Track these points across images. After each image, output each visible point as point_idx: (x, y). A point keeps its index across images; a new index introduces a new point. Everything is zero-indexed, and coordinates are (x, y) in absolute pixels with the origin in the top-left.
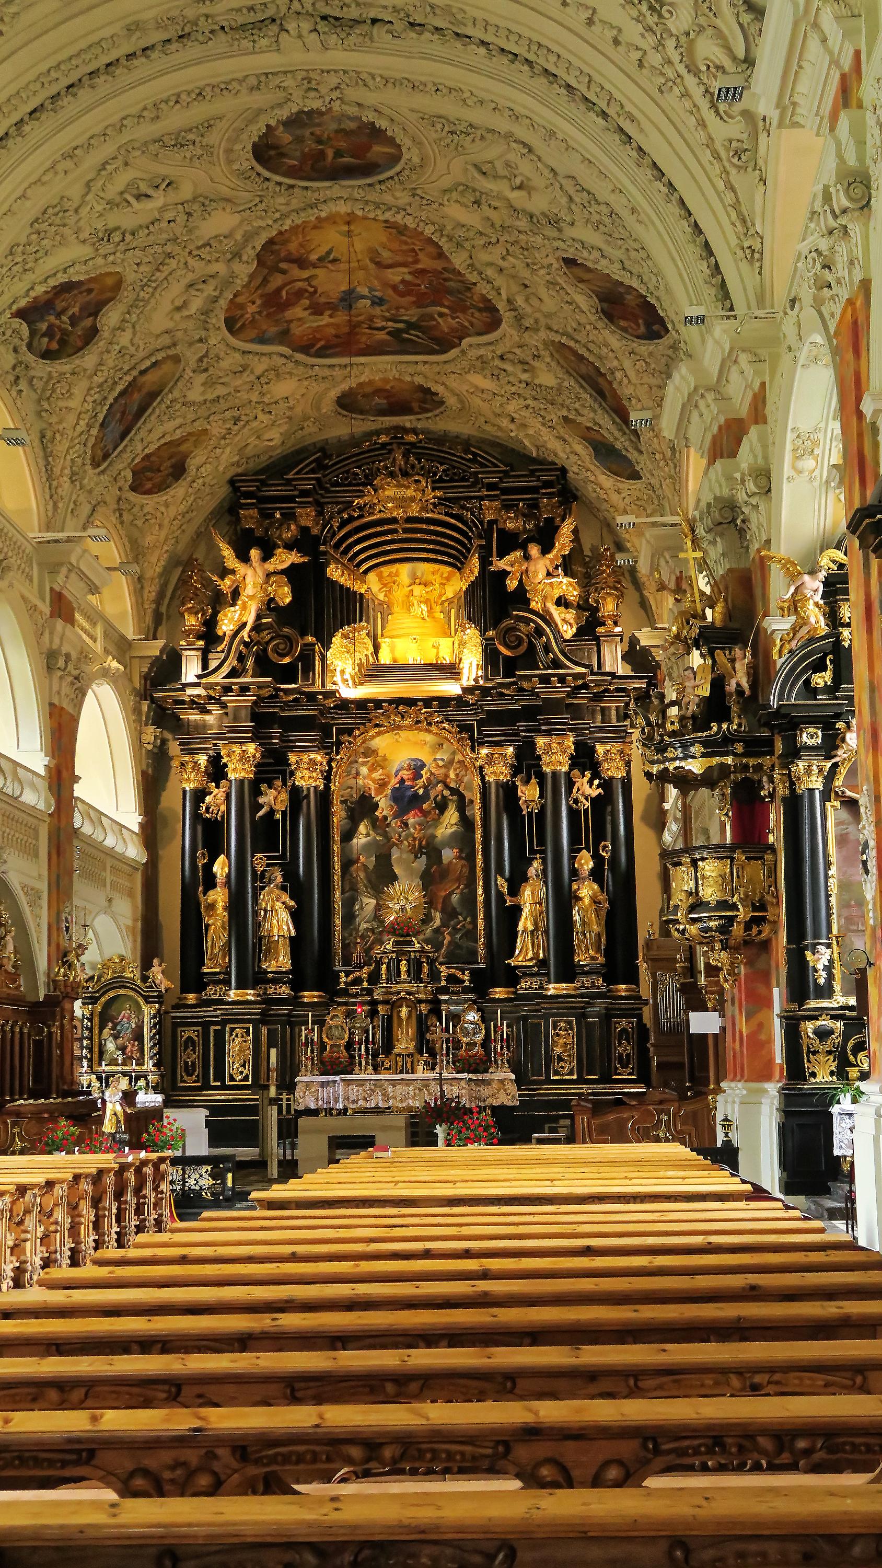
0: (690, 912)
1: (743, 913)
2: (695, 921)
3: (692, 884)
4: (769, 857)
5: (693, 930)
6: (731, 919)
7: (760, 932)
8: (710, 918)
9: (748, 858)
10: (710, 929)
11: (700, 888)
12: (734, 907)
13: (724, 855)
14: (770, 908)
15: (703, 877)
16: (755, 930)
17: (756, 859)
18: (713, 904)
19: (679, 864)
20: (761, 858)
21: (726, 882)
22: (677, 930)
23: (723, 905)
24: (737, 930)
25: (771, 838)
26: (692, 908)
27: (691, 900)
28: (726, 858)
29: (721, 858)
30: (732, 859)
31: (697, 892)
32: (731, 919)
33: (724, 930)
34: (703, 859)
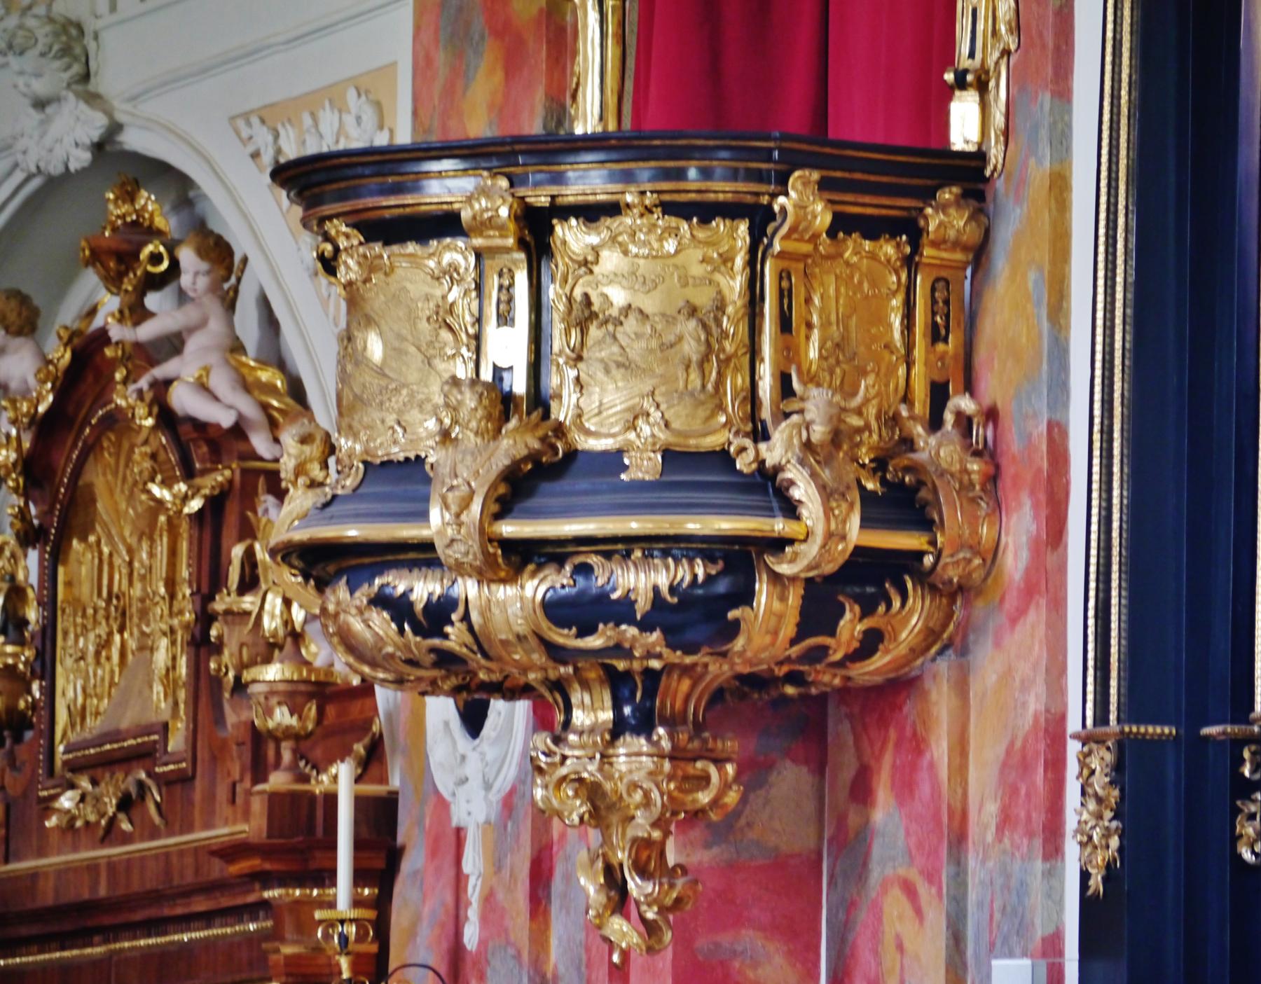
0: (504, 506)
1: (822, 526)
2: (522, 556)
3: (508, 348)
4: (945, 218)
5: (516, 601)
6: (740, 559)
7: (871, 642)
8: (618, 548)
9: (842, 225)
10: (622, 611)
11: (559, 378)
12: (768, 489)
13: (723, 190)
14: (953, 516)
15: (585, 315)
16: (851, 626)
17: (872, 228)
18: (644, 466)
19: (445, 224)
20: (909, 228)
21: (722, 350)
22: (399, 608)
23: (693, 470)
24: (768, 620)
25: (964, 124)
26: (518, 488)
27: (514, 443)
28: (731, 211)
29: (704, 212)
30: (761, 219)
31: (539, 400)
32: (740, 559)
33: (698, 618)
34: (591, 213)
